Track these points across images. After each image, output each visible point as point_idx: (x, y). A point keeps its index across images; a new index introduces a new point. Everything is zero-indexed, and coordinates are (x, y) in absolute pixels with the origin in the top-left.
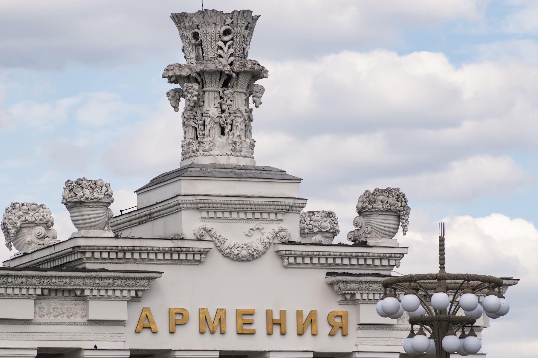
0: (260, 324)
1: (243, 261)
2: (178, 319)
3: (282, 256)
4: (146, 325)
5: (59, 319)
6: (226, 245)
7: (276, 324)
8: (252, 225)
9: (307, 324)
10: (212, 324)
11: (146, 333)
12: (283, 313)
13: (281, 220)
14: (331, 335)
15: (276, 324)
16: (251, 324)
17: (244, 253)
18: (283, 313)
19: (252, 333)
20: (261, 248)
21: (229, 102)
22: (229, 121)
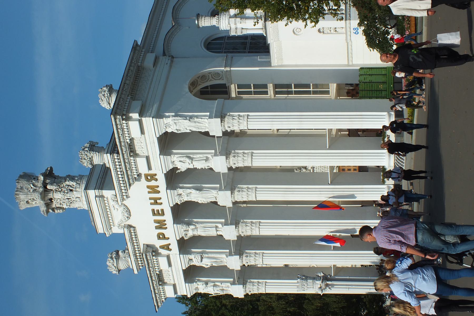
0: (156, 207)
1: (130, 213)
2: (161, 237)
3: (123, 200)
4: (167, 247)
5: (171, 274)
6: (124, 220)
7: (156, 202)
8: (112, 208)
9: (154, 190)
10: (161, 225)
11: (170, 247)
12: (150, 199)
13: (107, 199)
14: (156, 180)
15: (156, 202)
16: (158, 210)
17: (126, 215)
18: (150, 199)
19: (162, 210)
20: (122, 207)
21: (59, 200)
22: (67, 200)
